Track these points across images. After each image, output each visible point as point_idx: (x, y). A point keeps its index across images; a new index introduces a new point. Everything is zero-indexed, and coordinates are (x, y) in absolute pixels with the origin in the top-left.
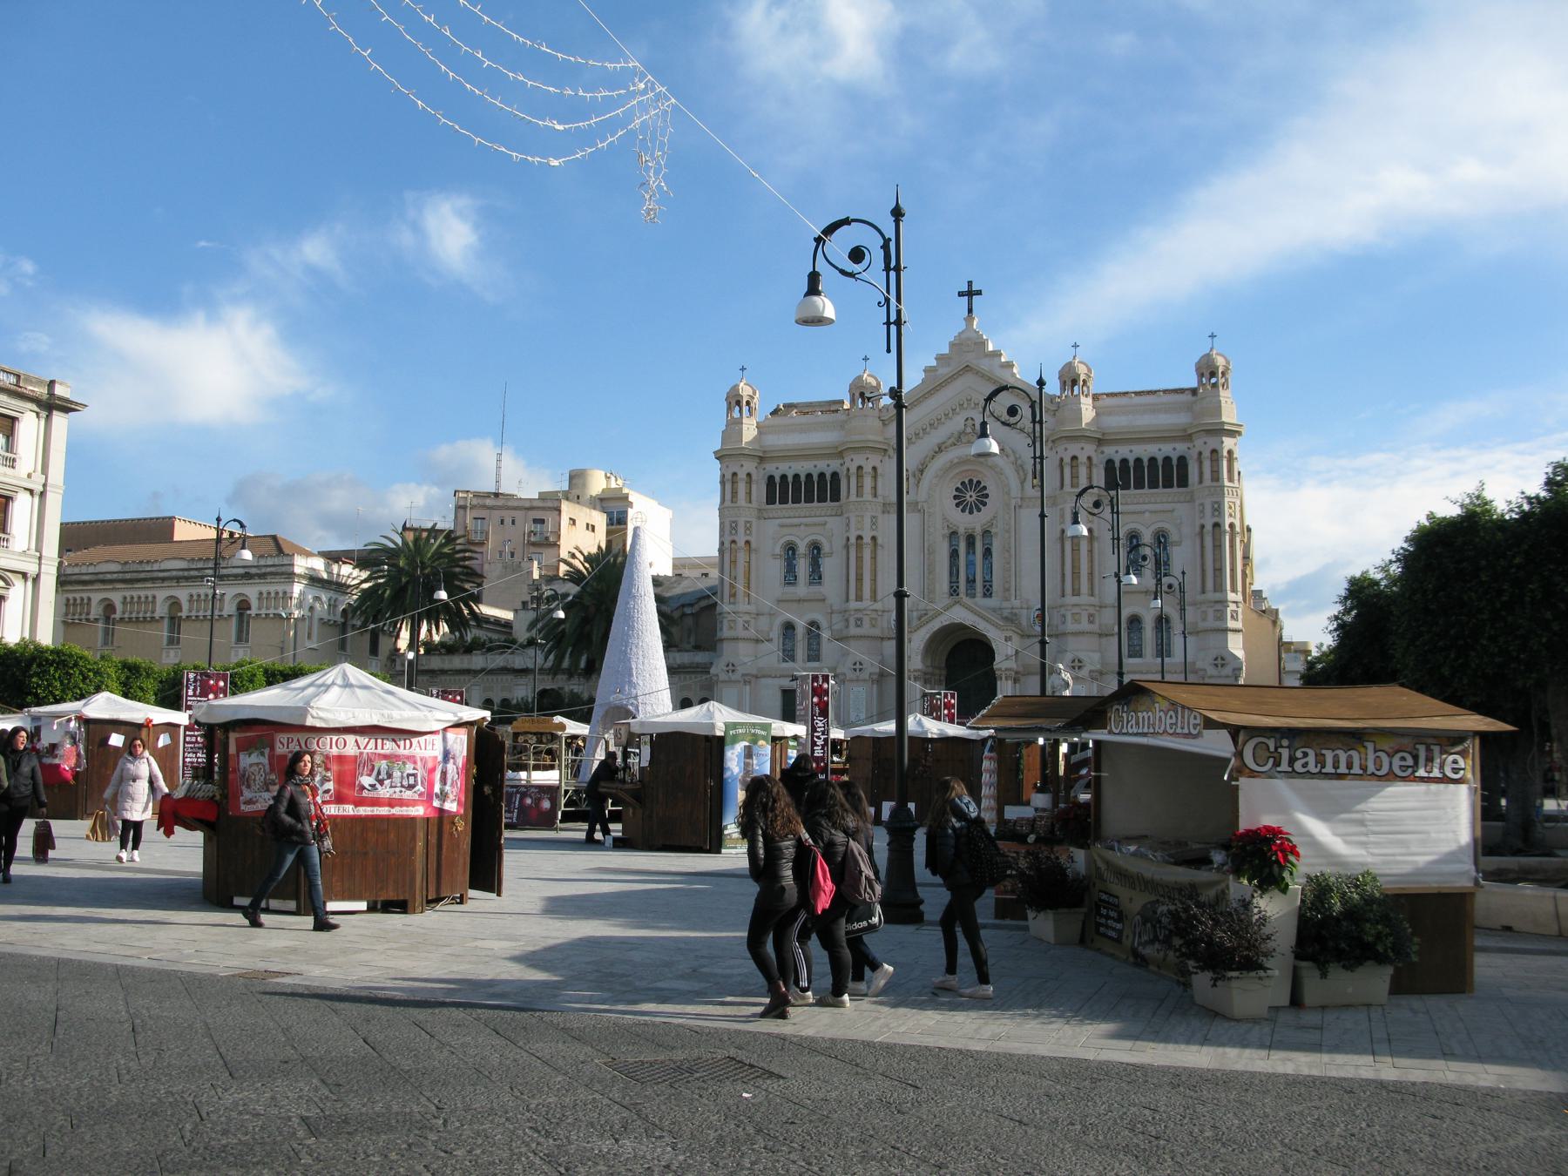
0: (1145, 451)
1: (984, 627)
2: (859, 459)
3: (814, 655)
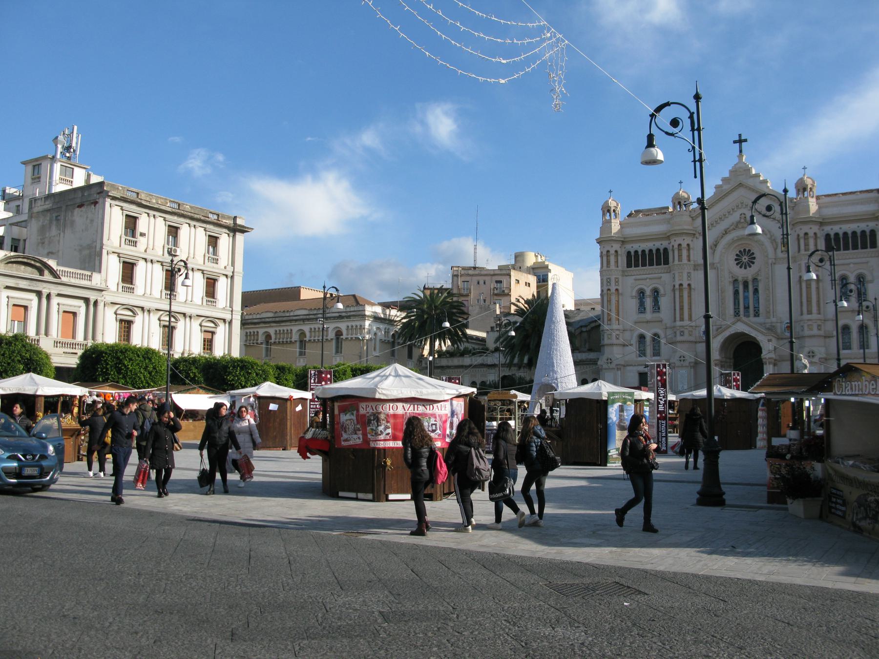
0: (849, 228)
1: (753, 334)
2: (679, 240)
3: (657, 353)
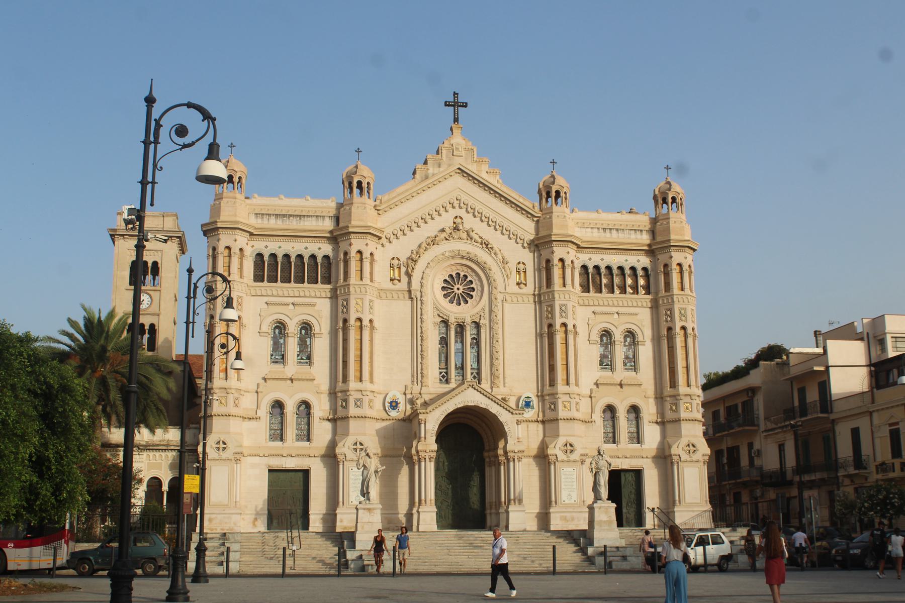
1: (494, 409)
